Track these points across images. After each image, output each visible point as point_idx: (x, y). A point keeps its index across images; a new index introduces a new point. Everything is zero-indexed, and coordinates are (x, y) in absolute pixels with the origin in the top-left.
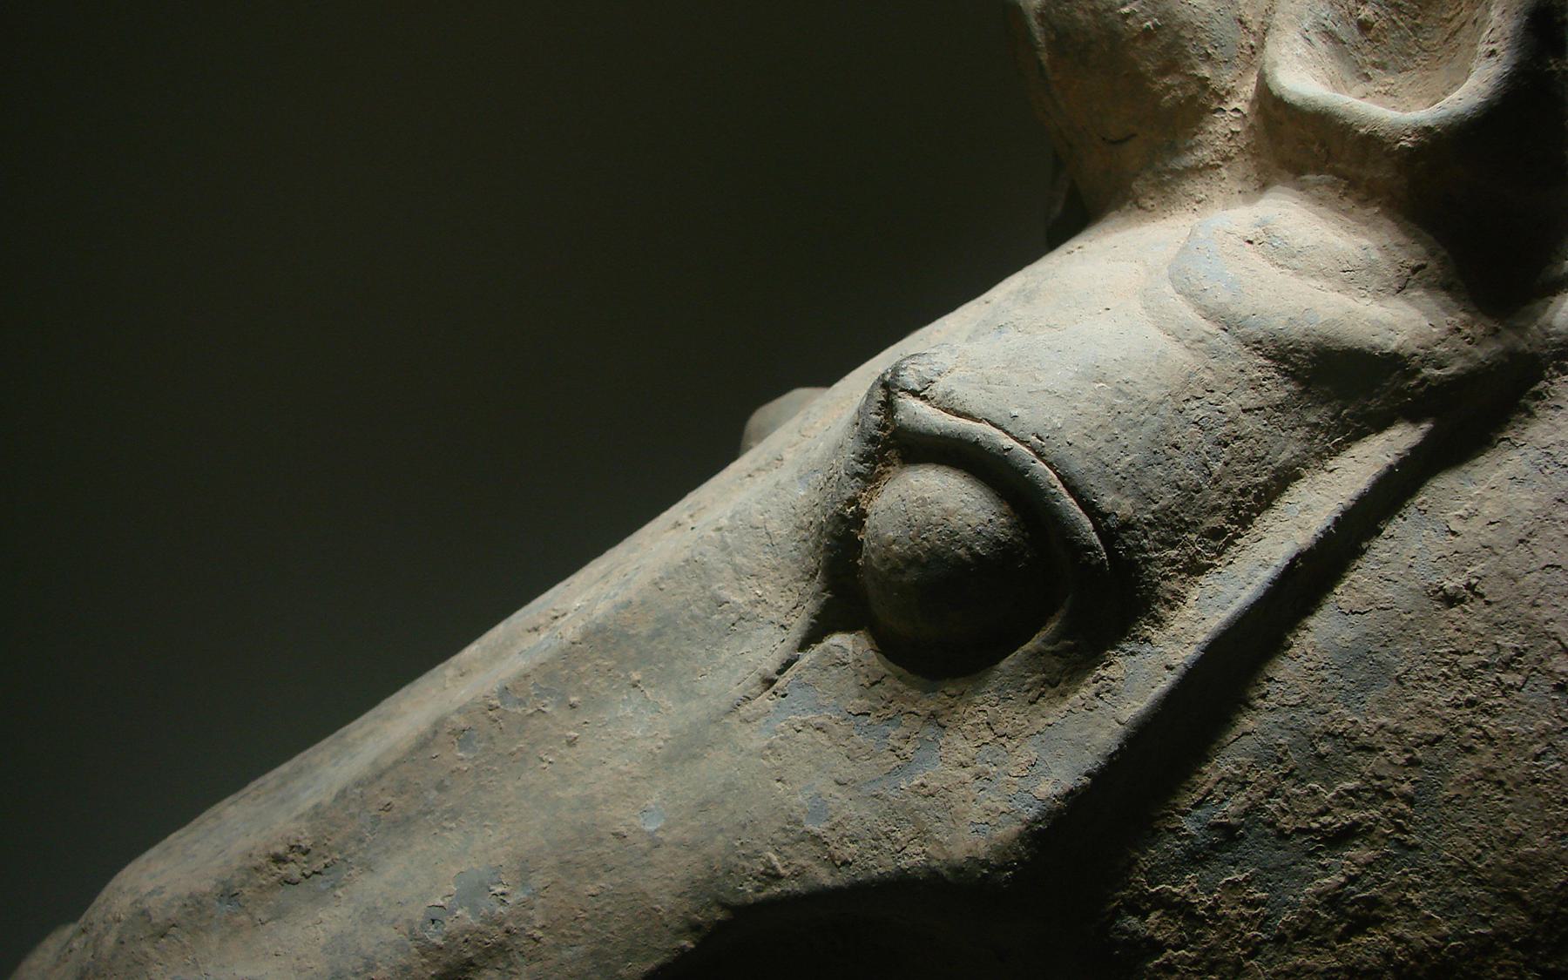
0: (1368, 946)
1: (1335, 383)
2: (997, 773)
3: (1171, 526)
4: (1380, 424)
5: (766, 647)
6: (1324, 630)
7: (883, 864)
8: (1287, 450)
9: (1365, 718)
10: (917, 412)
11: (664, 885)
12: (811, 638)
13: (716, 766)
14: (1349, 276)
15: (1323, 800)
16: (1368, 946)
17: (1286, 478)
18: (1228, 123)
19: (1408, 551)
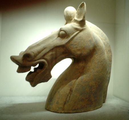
0: (77, 49)
1: (77, 29)
2: (64, 41)
3: (71, 34)
4: (77, 31)
5: (56, 38)
6: (76, 38)
7: (60, 45)
8: (74, 32)
9: (77, 41)
10: (62, 29)
11: (52, 46)
12: (58, 37)
13: (54, 42)
14: (77, 26)
15: (75, 44)
16: (77, 49)
17: (74, 33)
18: (73, 20)
19: (78, 35)
